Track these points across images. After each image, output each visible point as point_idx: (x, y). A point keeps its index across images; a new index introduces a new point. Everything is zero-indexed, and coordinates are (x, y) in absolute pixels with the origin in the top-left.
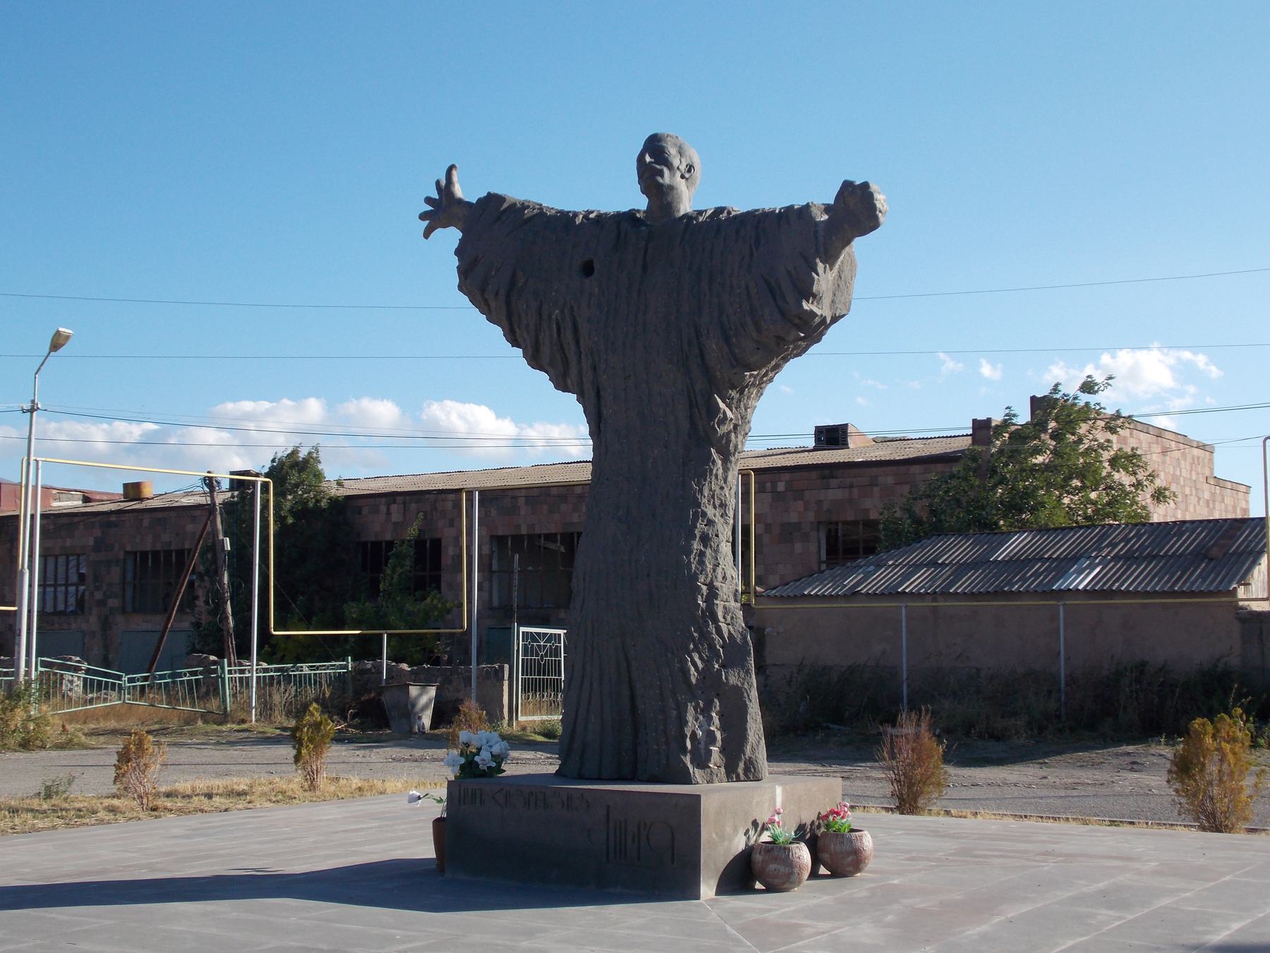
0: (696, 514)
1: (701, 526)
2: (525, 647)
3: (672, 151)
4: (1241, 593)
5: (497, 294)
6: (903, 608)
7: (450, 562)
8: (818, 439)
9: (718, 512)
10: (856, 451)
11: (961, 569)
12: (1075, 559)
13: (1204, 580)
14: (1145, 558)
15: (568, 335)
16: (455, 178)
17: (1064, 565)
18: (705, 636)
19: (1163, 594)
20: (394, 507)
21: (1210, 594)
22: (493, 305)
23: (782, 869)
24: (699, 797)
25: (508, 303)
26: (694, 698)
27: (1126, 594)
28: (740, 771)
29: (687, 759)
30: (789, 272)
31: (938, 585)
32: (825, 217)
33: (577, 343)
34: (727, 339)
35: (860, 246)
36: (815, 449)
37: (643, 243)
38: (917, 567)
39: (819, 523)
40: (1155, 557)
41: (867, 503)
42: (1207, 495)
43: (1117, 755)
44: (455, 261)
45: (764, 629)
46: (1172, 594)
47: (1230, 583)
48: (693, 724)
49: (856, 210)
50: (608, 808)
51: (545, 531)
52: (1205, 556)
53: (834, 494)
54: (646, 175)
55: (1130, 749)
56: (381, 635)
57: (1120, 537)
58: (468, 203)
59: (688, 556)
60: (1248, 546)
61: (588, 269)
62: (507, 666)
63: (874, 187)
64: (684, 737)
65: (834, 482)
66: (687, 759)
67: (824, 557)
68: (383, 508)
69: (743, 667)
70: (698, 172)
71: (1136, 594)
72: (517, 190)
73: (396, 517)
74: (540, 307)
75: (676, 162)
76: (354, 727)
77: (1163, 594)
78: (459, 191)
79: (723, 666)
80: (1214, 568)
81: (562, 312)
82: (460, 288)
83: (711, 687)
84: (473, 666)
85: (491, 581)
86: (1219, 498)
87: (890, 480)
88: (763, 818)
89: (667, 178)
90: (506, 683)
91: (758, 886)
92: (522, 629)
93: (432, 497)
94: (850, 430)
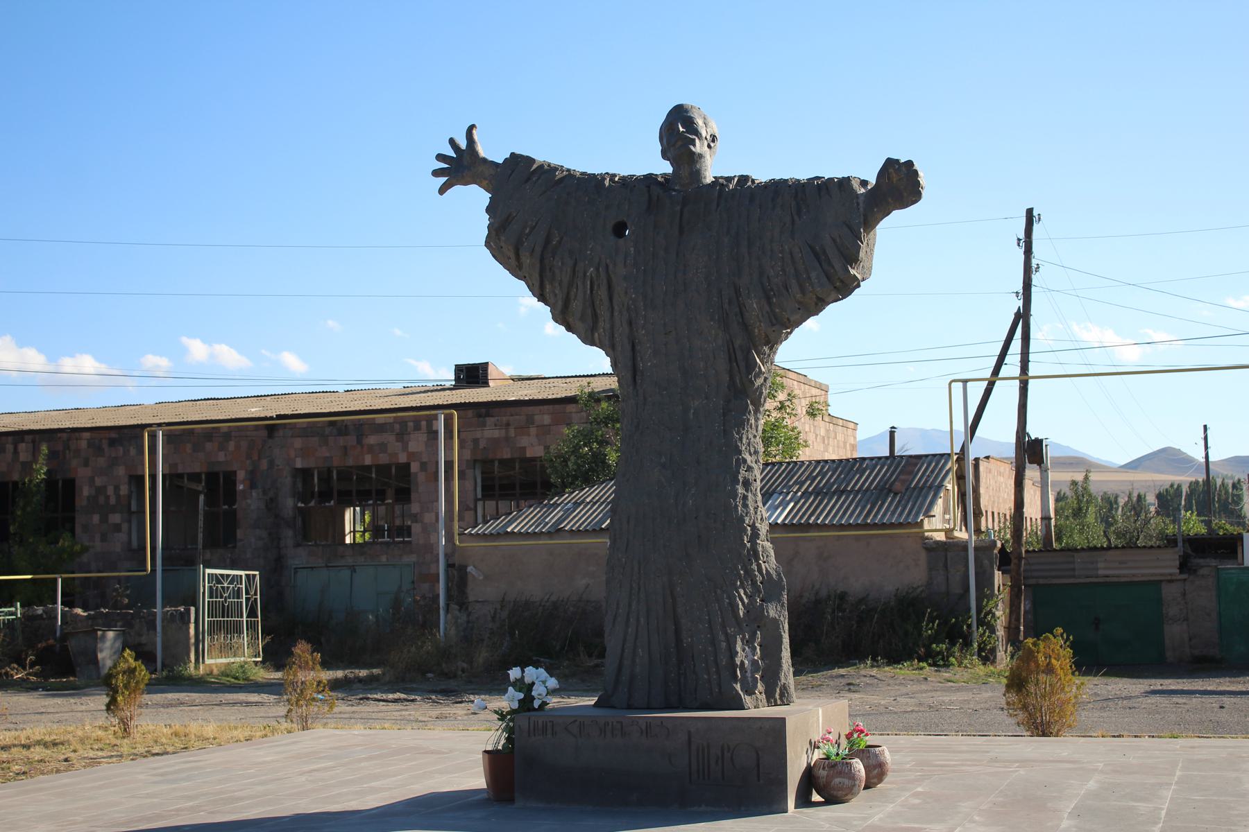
0: (738, 460)
1: (743, 473)
2: (210, 588)
3: (700, 122)
4: (926, 526)
7: (84, 503)
8: (457, 379)
9: (754, 458)
14: (834, 493)
15: (603, 293)
16: (476, 137)
18: (749, 573)
19: (857, 526)
20: (22, 446)
21: (900, 525)
22: (526, 260)
23: (846, 781)
24: (784, 720)
25: (542, 260)
26: (741, 631)
28: (777, 696)
29: (738, 687)
30: (834, 240)
32: (863, 191)
33: (611, 299)
34: (768, 299)
35: (897, 217)
36: (455, 388)
37: (678, 208)
39: (475, 461)
40: (843, 492)
41: (524, 441)
42: (823, 432)
43: (832, 677)
44: (485, 220)
45: (466, 567)
46: (865, 526)
47: (917, 515)
48: (742, 655)
49: (899, 185)
50: (689, 733)
51: (189, 470)
52: (890, 491)
53: (491, 432)
54: (680, 143)
55: (842, 671)
56: (55, 580)
57: (807, 474)
59: (735, 500)
60: (926, 481)
61: (619, 229)
62: (193, 609)
63: (917, 166)
64: (734, 666)
65: (490, 421)
66: (738, 687)
67: (479, 496)
68: (10, 447)
69: (779, 601)
70: (718, 143)
71: (831, 527)
72: (543, 152)
73: (23, 457)
74: (575, 264)
75: (704, 134)
76: (35, 675)
78: (482, 151)
79: (762, 600)
80: (899, 502)
81: (597, 269)
82: (487, 244)
83: (756, 619)
84: (158, 610)
85: (130, 522)
86: (832, 435)
87: (547, 419)
88: (816, 737)
89: (699, 147)
90: (192, 626)
92: (208, 571)
93: (65, 435)
94: (490, 369)
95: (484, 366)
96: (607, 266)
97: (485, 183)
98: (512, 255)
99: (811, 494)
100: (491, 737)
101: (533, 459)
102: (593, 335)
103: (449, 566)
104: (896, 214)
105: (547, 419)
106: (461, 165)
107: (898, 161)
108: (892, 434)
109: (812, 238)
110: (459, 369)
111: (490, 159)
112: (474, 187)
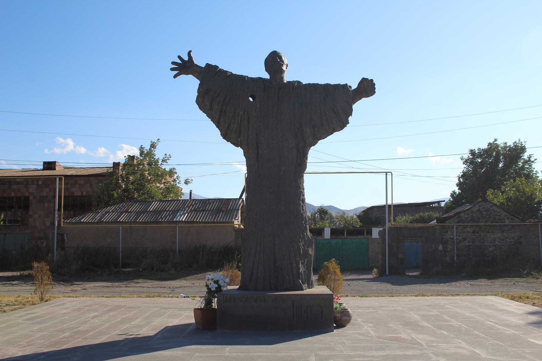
6: (121, 226)
10: (58, 171)
11: (139, 214)
12: (178, 211)
13: (223, 218)
17: (175, 212)
18: (304, 236)
19: (211, 223)
21: (226, 222)
23: (348, 318)
27: (199, 222)
31: (132, 219)
38: (122, 213)
46: (214, 222)
47: (232, 219)
49: (367, 88)
52: (221, 210)
77: (211, 223)
87: (82, 182)
89: (284, 68)
91: (335, 325)
94: (57, 164)
95: (54, 163)
97: (197, 74)
99: (193, 211)
100: (199, 303)
101: (77, 196)
103: (58, 234)
104: (364, 99)
105: (82, 182)
106: (185, 67)
108: (191, 193)
109: (329, 107)
110: (45, 163)
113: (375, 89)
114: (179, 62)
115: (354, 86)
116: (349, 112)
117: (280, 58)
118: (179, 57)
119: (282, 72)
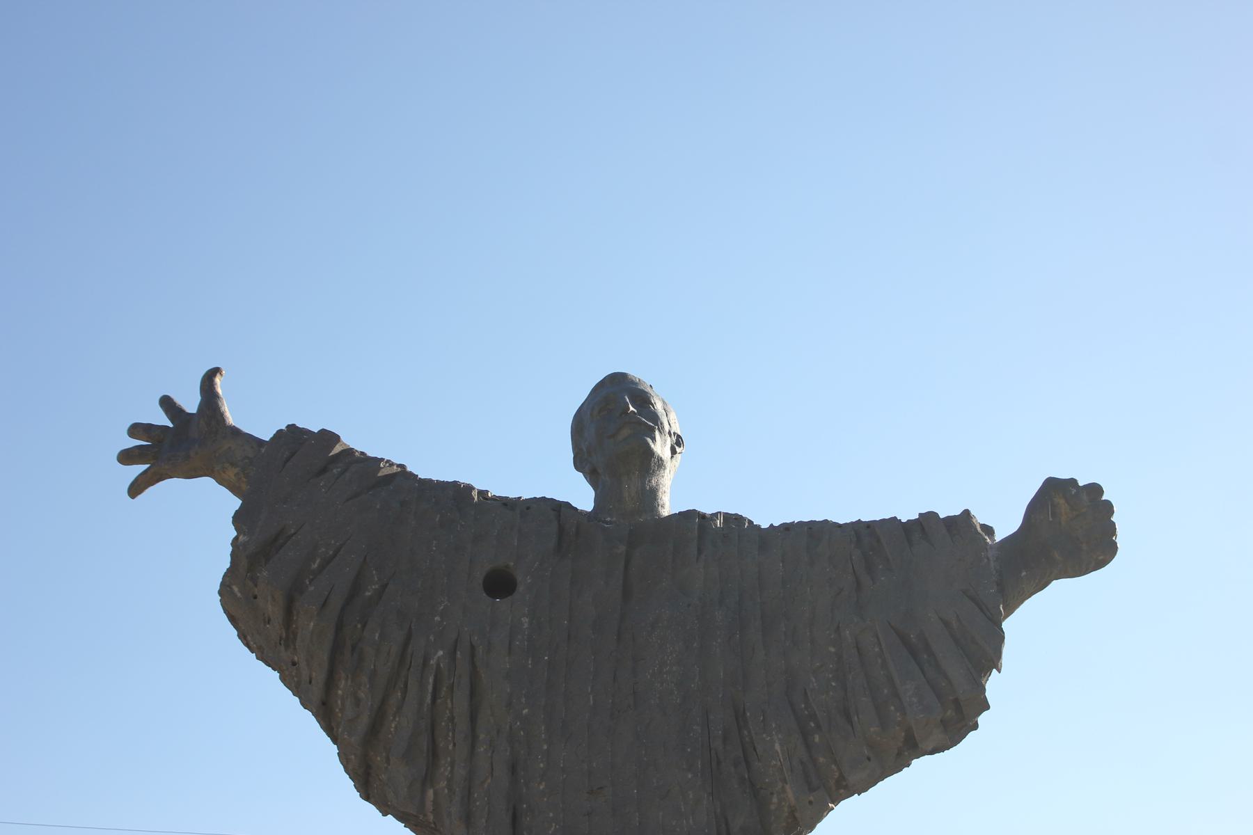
3: (659, 407)
5: (324, 604)
22: (307, 624)
25: (339, 627)
30: (947, 624)
37: (622, 548)
49: (1071, 530)
58: (250, 438)
82: (226, 591)
89: (661, 447)
96: (473, 647)
97: (231, 473)
98: (273, 609)
102: (423, 792)
104: (1060, 588)
106: (181, 442)
107: (1073, 482)
111: (246, 429)
112: (207, 483)
113: (1111, 529)
114: (162, 420)
115: (1004, 518)
116: (986, 655)
117: (643, 399)
118: (167, 404)
119: (648, 464)
